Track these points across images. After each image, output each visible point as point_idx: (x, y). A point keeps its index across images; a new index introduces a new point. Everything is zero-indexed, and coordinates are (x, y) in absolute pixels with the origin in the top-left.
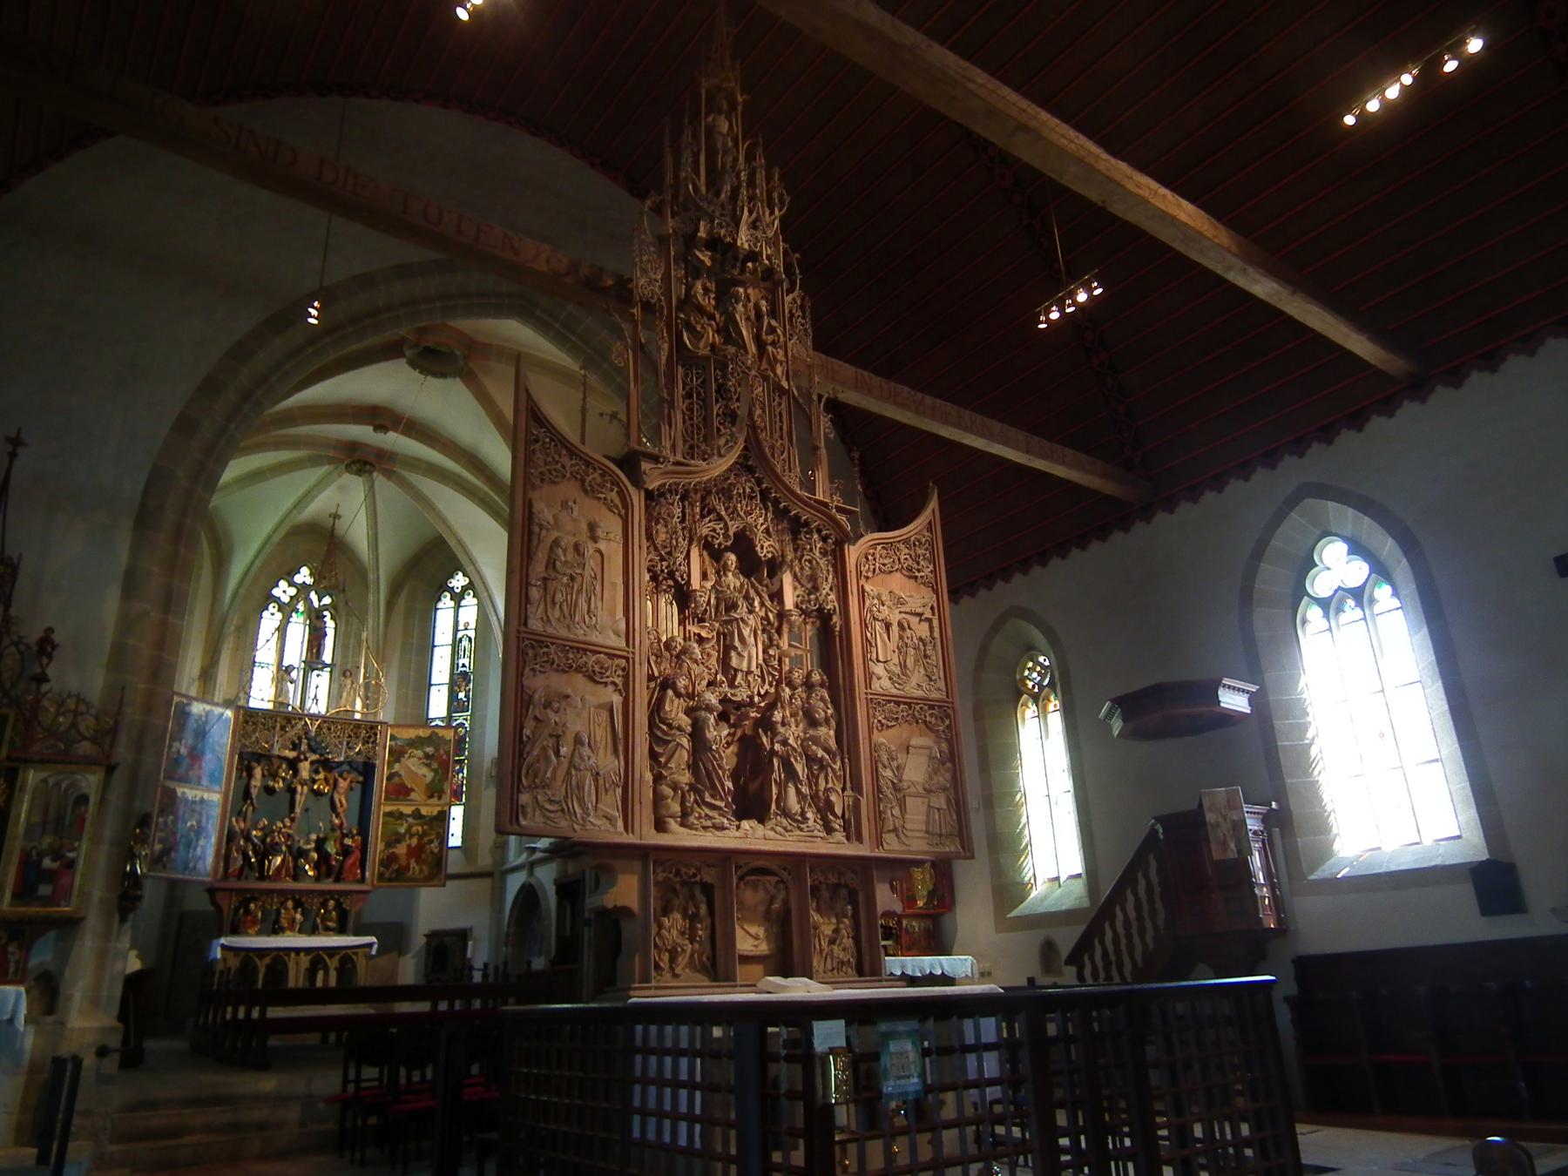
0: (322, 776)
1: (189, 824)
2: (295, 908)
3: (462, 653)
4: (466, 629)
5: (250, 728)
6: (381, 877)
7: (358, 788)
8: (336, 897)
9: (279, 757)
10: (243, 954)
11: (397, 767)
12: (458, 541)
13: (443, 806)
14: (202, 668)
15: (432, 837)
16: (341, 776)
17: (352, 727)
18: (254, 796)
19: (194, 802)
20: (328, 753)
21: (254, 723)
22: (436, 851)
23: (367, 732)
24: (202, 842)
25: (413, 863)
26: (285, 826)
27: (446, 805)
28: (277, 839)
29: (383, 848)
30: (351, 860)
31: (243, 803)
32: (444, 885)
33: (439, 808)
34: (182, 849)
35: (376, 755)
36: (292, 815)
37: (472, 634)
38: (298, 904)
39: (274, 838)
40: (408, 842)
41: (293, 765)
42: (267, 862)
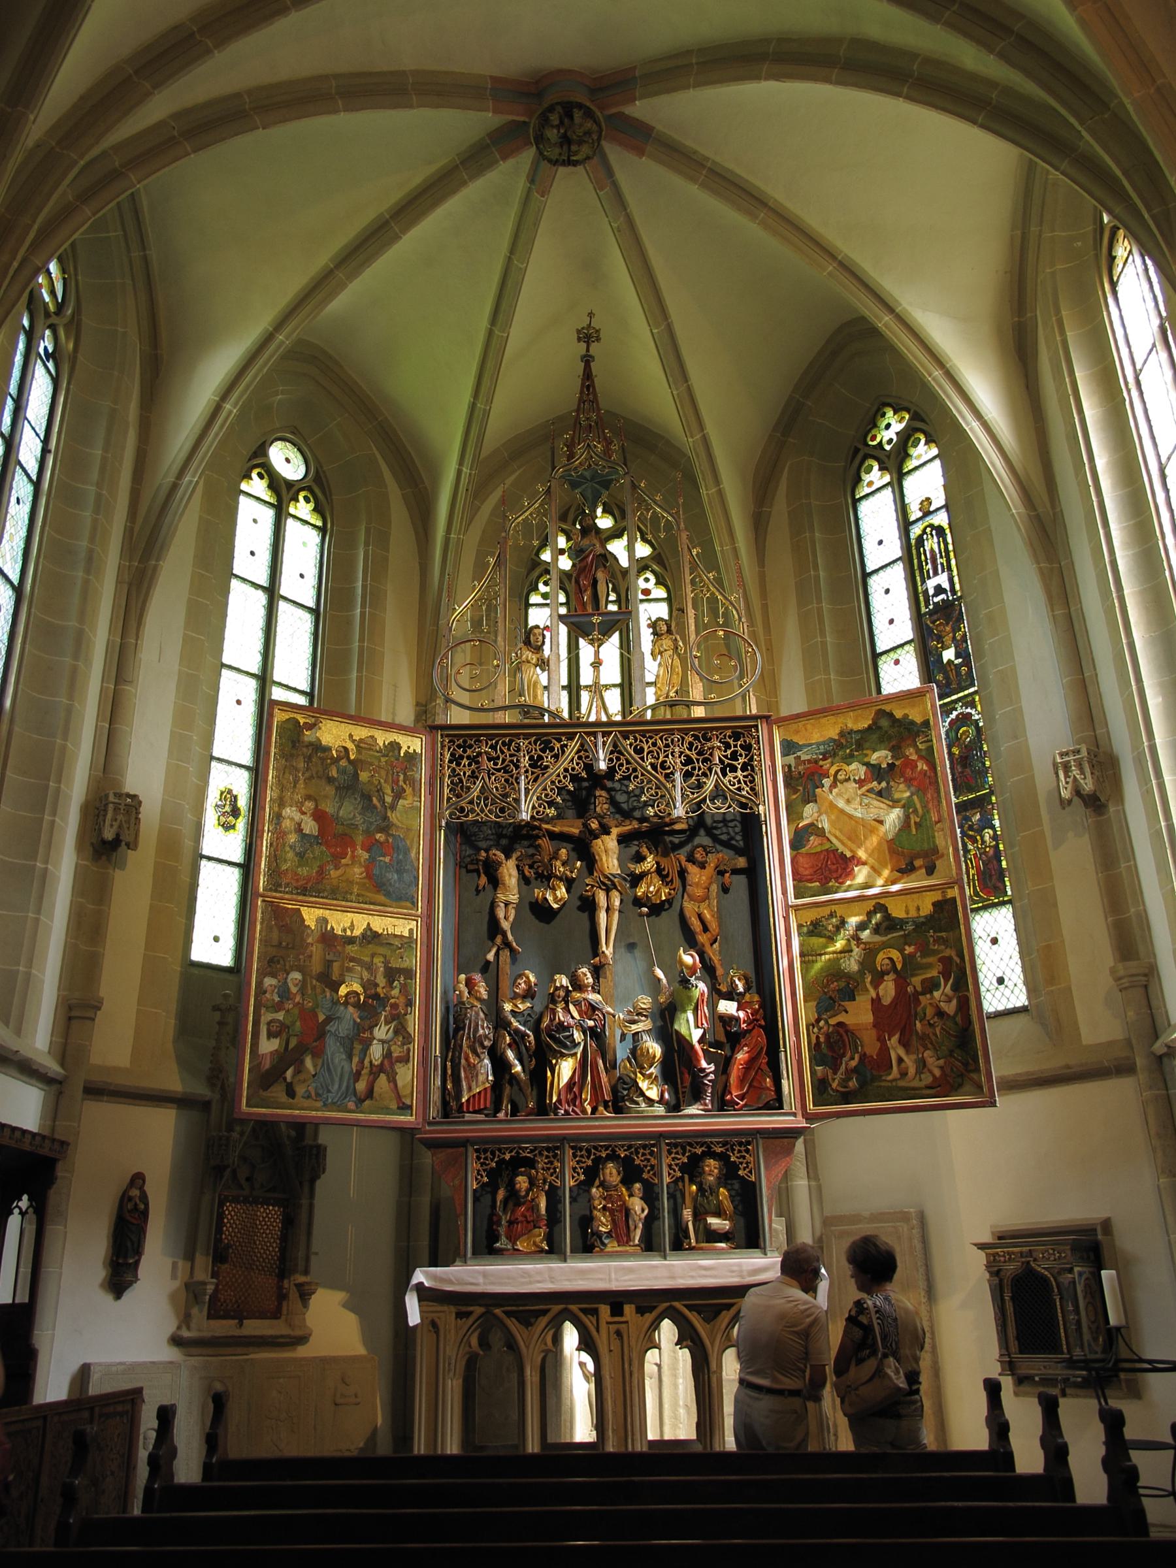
0: (650, 863)
1: (343, 990)
2: (627, 1181)
3: (929, 566)
4: (927, 513)
5: (465, 769)
6: (821, 1086)
7: (740, 884)
8: (719, 1150)
9: (553, 836)
10: (479, 1310)
11: (809, 812)
12: (841, 264)
13: (943, 888)
14: (418, 704)
15: (933, 973)
16: (691, 859)
17: (689, 739)
18: (506, 925)
19: (351, 940)
20: (646, 804)
21: (474, 760)
22: (950, 1008)
23: (728, 746)
24: (382, 1032)
25: (896, 1050)
26: (578, 986)
27: (950, 885)
28: (561, 1015)
29: (814, 1016)
30: (741, 1056)
31: (491, 944)
32: (993, 1104)
33: (937, 896)
34: (331, 1045)
35: (755, 794)
36: (598, 959)
37: (941, 519)
38: (631, 1175)
39: (554, 1012)
40: (873, 994)
41: (583, 849)
42: (549, 1074)
